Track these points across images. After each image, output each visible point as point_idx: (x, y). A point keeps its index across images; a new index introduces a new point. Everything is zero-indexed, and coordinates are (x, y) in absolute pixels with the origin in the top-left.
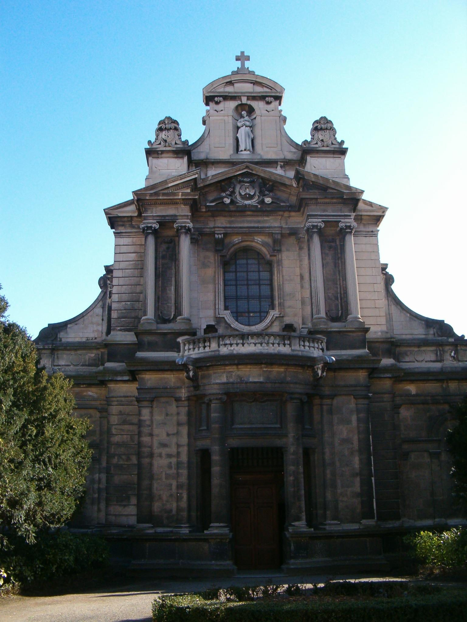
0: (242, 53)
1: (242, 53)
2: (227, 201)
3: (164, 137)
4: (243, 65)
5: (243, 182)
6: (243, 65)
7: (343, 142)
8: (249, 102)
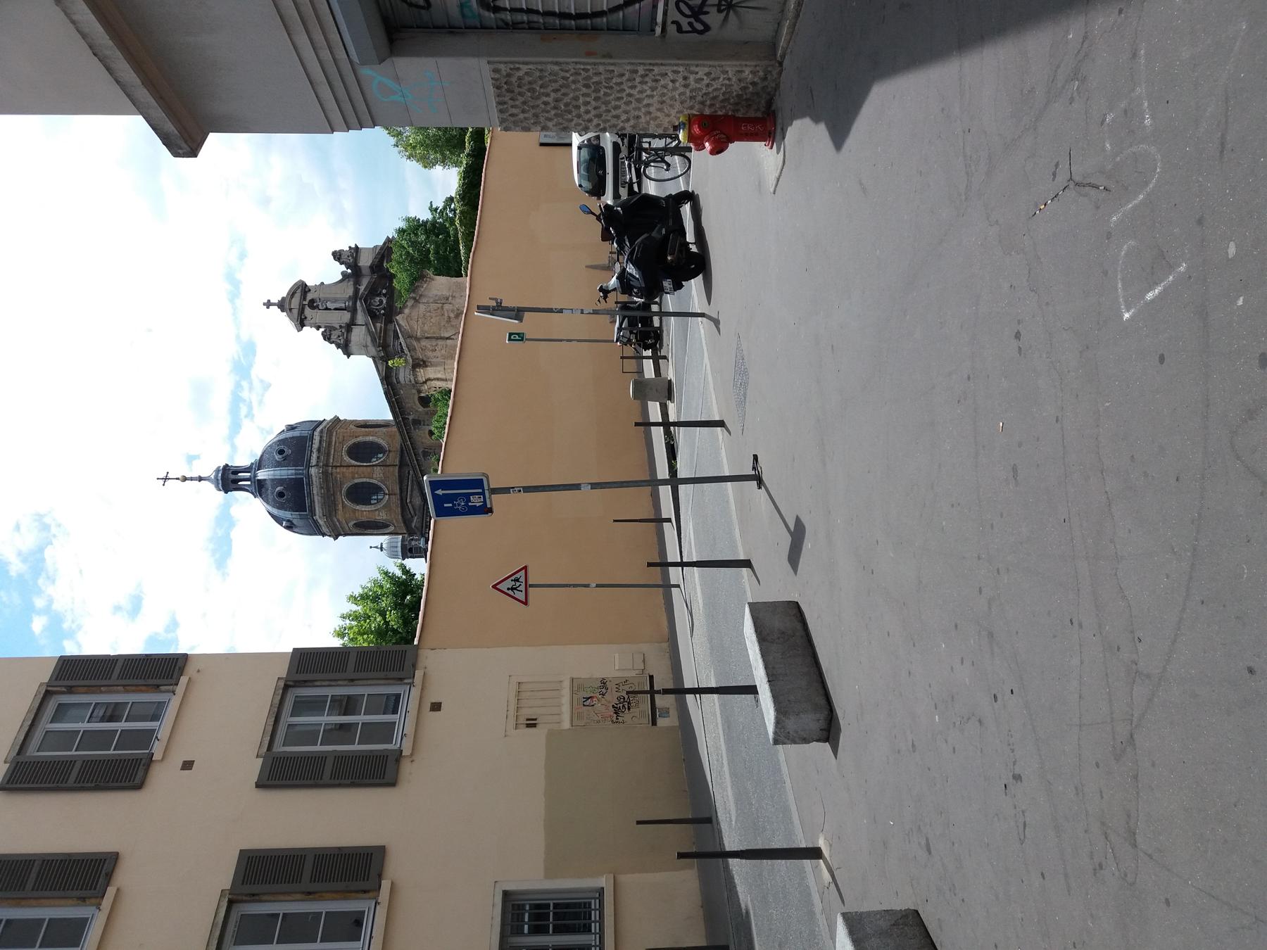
0: (264, 304)
1: (264, 304)
2: (383, 312)
3: (335, 337)
4: (274, 304)
5: (370, 302)
6: (274, 304)
7: (350, 247)
8: (308, 300)
